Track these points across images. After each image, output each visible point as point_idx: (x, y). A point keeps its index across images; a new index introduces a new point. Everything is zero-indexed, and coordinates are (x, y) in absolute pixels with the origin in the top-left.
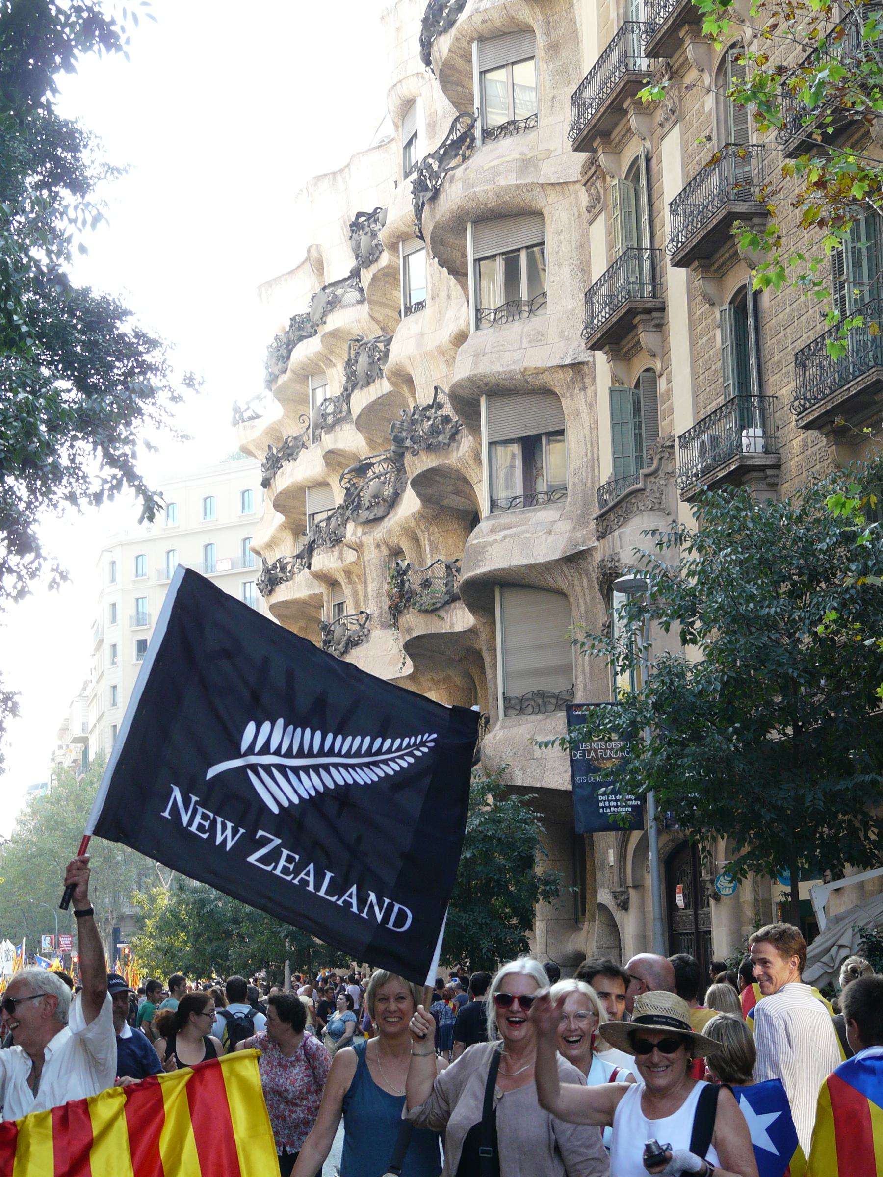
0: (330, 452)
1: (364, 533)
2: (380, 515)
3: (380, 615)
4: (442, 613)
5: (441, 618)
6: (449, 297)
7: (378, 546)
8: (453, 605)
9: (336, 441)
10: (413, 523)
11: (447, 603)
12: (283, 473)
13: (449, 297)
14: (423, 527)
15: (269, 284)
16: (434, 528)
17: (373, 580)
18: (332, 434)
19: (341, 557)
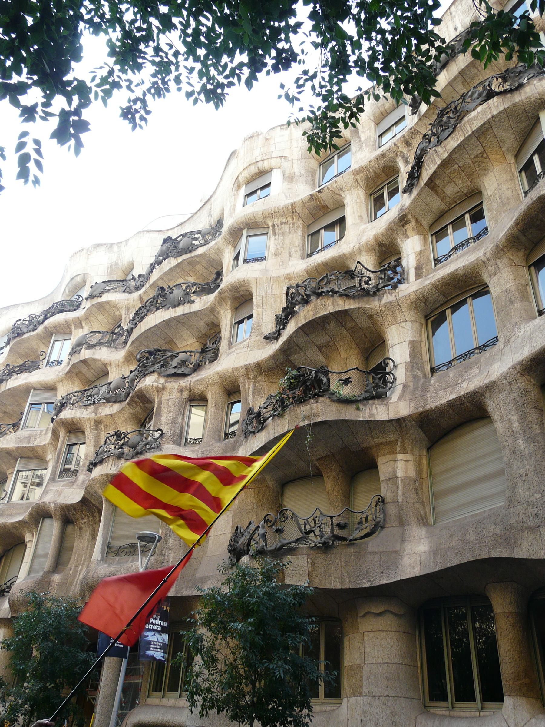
0: (84, 361)
1: (166, 382)
2: (186, 372)
3: (173, 435)
4: (361, 406)
5: (358, 409)
6: (290, 256)
7: (181, 391)
8: (370, 402)
9: (93, 354)
10: (243, 371)
11: (366, 399)
12: (17, 378)
13: (290, 256)
14: (251, 376)
15: (7, 308)
16: (262, 378)
17: (170, 412)
18: (92, 351)
19: (96, 412)
